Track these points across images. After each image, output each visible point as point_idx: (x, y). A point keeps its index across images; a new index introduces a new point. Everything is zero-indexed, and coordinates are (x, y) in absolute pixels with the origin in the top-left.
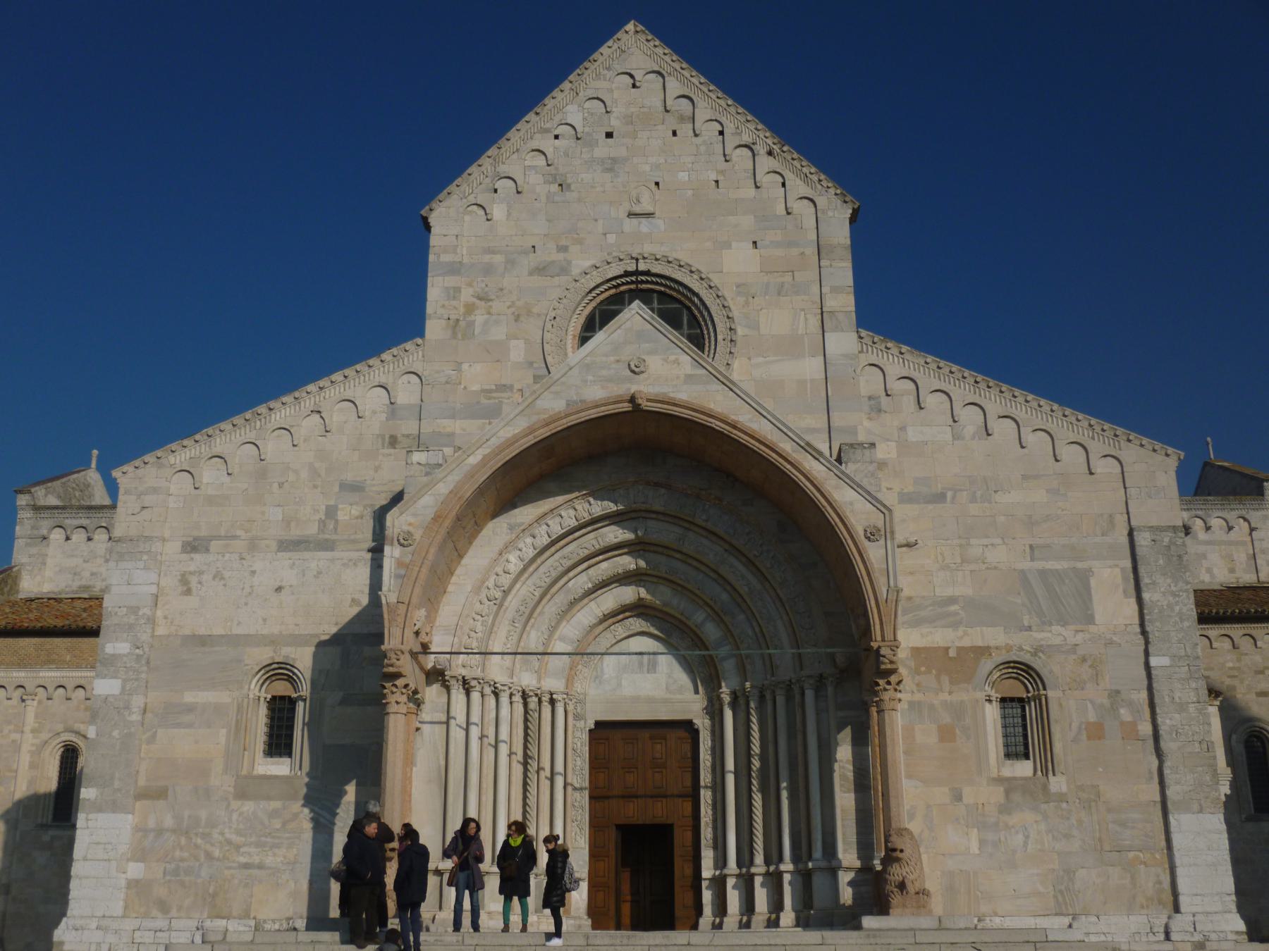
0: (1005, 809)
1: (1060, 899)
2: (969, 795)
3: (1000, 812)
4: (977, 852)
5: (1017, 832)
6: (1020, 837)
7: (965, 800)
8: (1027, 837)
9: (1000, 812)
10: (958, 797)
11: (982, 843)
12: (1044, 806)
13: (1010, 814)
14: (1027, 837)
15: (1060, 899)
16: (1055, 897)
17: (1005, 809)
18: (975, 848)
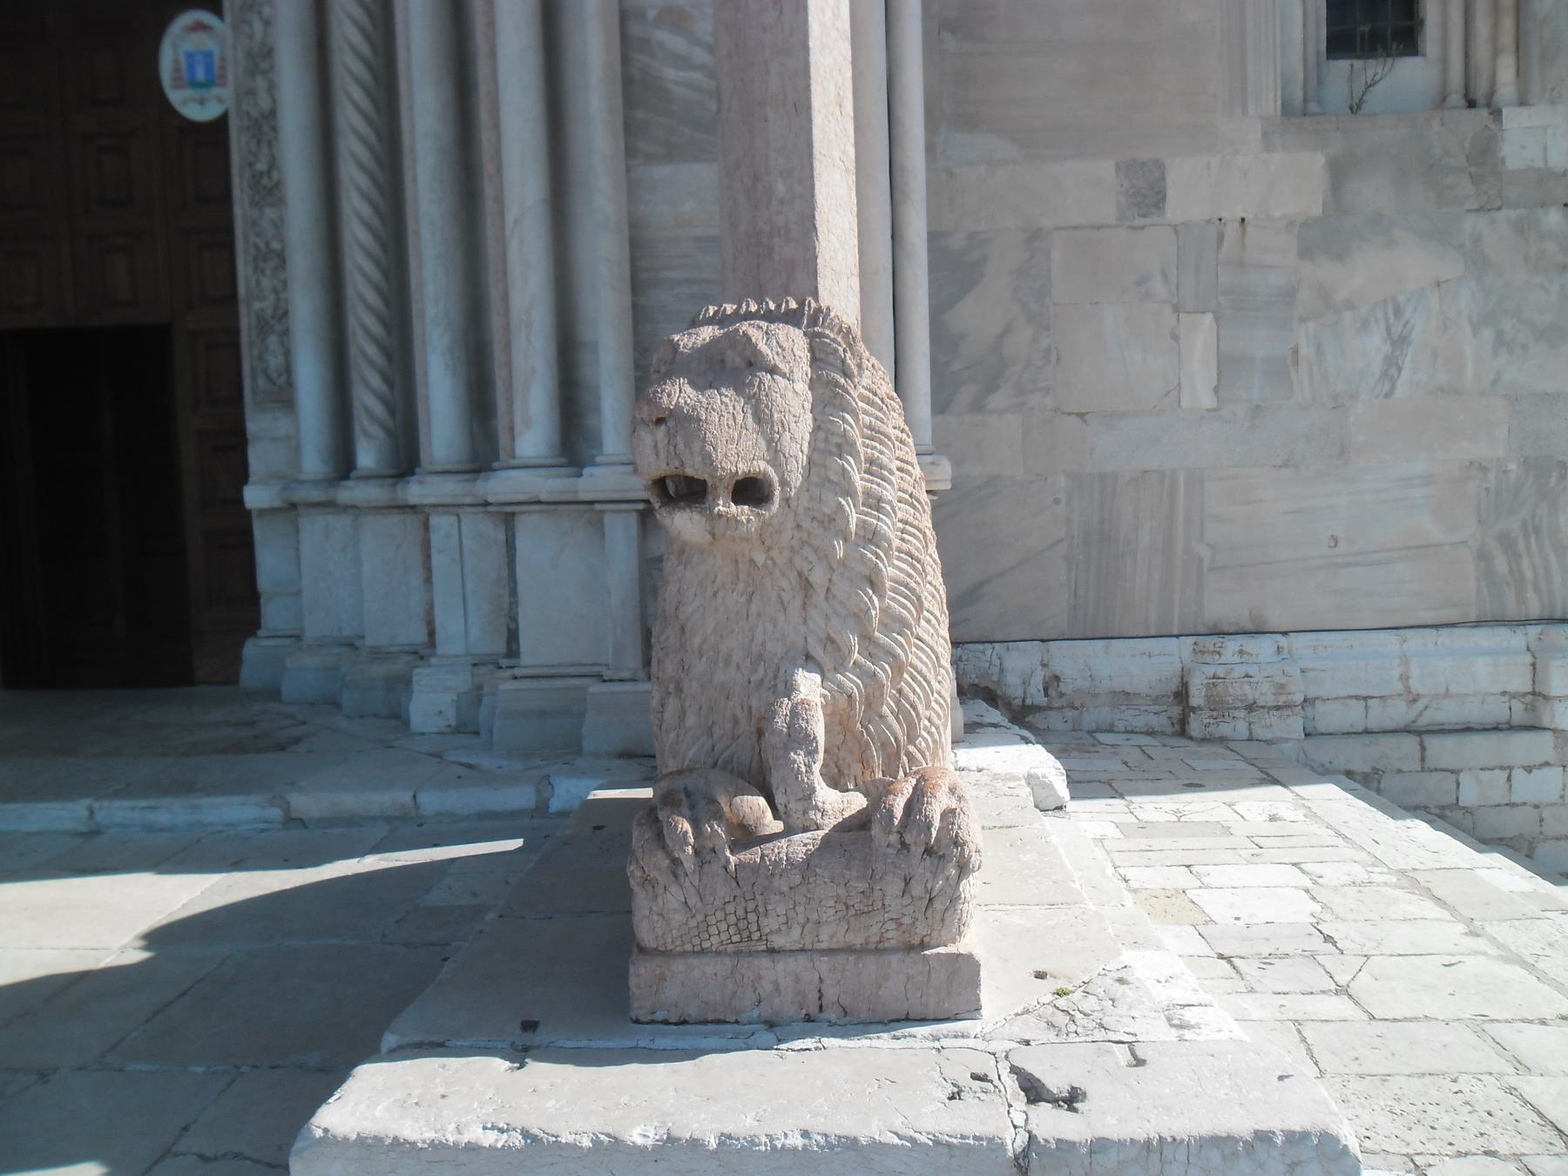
0: (1325, 237)
1: (1501, 565)
2: (1192, 191)
3: (1305, 252)
4: (1208, 401)
5: (1365, 325)
6: (1374, 345)
7: (1175, 210)
8: (1399, 342)
9: (1305, 252)
10: (1148, 195)
11: (1228, 366)
12: (1470, 224)
13: (1340, 257)
14: (1399, 342)
15: (1501, 565)
16: (1483, 556)
17: (1325, 237)
18: (1200, 390)
